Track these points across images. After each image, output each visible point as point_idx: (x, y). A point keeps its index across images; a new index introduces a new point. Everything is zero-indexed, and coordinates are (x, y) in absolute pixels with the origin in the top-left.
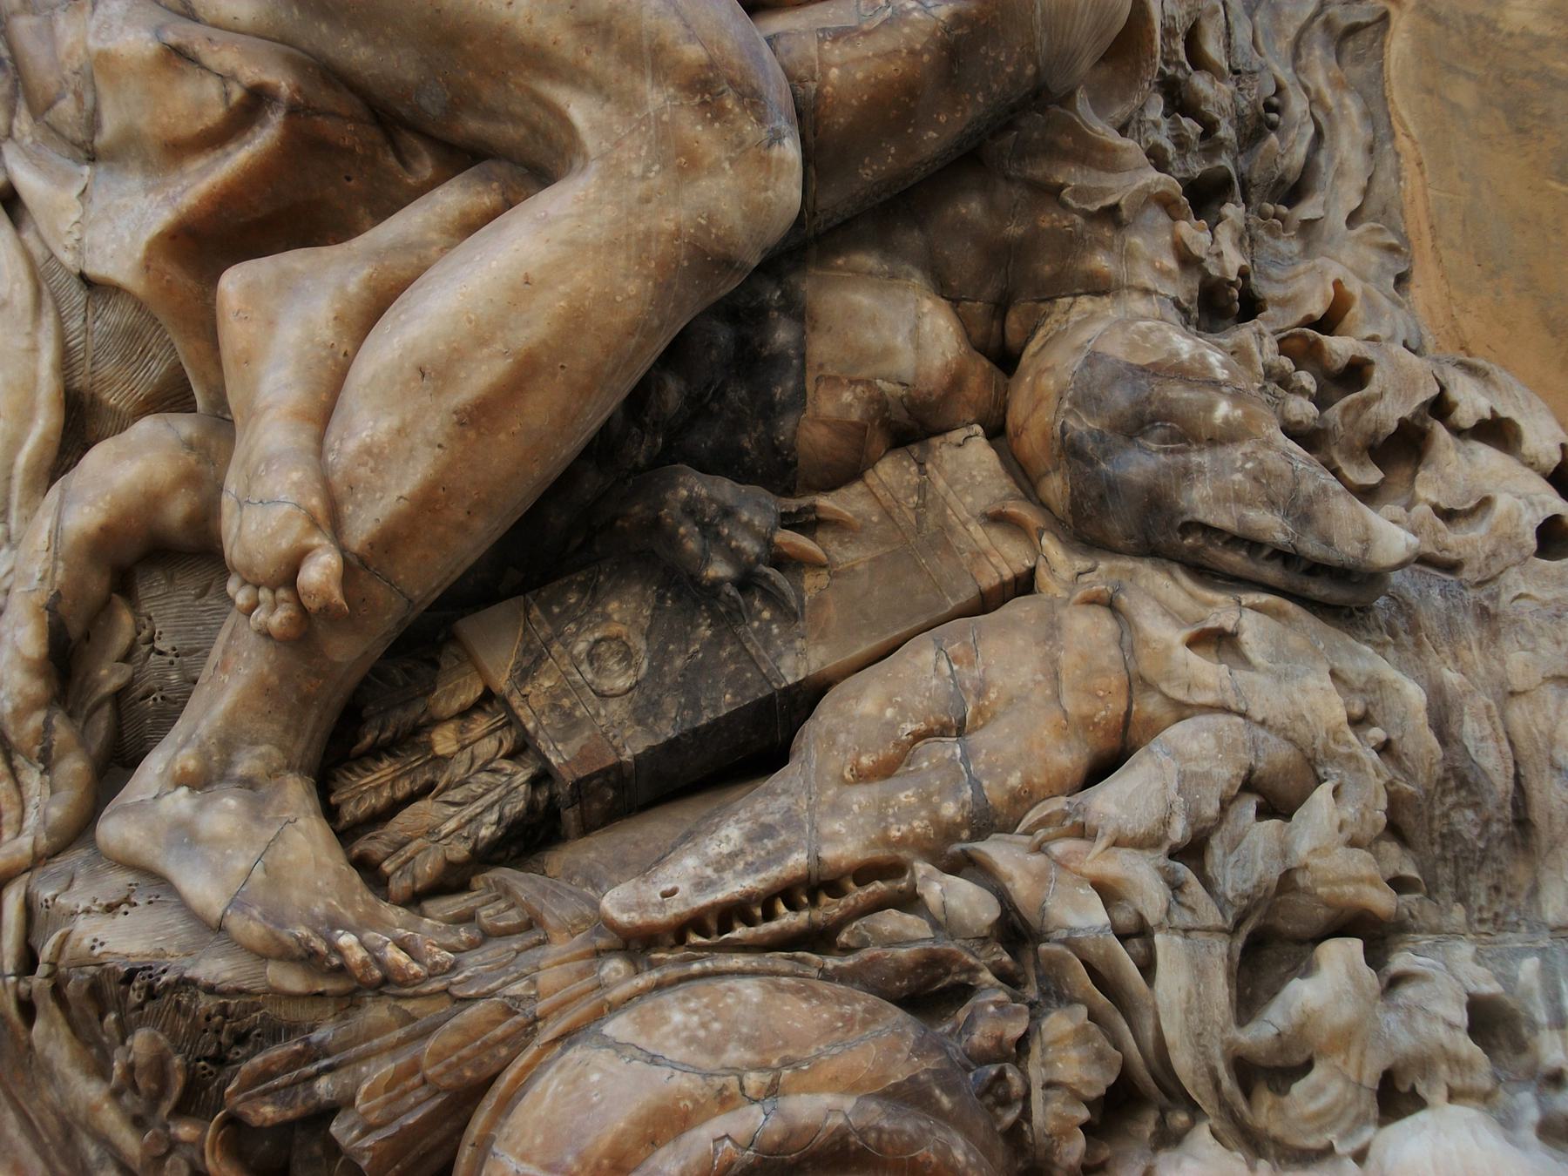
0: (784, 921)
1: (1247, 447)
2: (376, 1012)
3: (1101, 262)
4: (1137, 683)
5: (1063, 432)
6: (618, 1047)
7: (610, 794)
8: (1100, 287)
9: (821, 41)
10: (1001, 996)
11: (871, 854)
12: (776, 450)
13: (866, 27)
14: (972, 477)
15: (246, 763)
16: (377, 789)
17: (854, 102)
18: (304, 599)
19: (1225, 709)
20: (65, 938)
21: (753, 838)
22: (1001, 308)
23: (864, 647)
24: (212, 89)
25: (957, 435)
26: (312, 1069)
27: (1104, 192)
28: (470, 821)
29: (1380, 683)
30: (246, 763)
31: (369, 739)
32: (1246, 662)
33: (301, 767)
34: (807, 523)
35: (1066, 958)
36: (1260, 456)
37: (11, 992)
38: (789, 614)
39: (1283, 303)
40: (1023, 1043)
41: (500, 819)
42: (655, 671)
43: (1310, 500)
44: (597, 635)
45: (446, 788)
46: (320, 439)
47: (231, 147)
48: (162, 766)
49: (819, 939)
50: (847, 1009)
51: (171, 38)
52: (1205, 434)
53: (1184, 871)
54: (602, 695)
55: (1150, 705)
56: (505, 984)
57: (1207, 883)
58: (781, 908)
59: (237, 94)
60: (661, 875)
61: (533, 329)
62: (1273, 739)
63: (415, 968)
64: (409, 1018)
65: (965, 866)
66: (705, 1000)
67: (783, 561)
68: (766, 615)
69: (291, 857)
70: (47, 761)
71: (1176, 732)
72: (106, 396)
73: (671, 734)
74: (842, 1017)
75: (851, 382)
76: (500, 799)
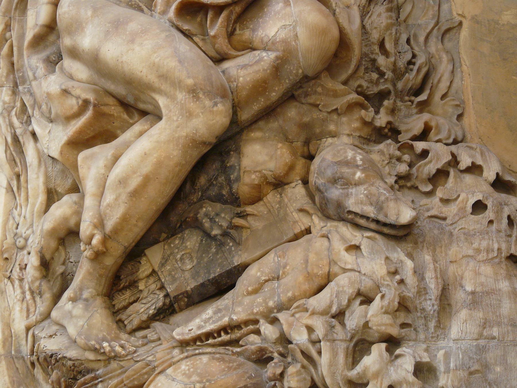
2: (114, 365)
3: (332, 127)
4: (332, 262)
7: (186, 300)
8: (334, 135)
9: (238, 69)
11: (248, 318)
12: (233, 194)
13: (251, 63)
15: (86, 294)
17: (248, 88)
21: (215, 313)
23: (258, 253)
25: (293, 185)
26: (97, 382)
28: (147, 308)
29: (402, 261)
30: (86, 294)
31: (122, 286)
33: (102, 295)
34: (243, 216)
35: (295, 349)
39: (407, 131)
40: (282, 375)
42: (199, 263)
44: (183, 253)
45: (142, 299)
47: (81, 117)
51: (63, 87)
52: (353, 183)
53: (334, 321)
54: (183, 270)
55: (335, 269)
56: (148, 357)
59: (80, 102)
61: (146, 169)
62: (367, 280)
64: (122, 367)
65: (274, 321)
67: (237, 228)
69: (94, 321)
70: (41, 294)
73: (202, 281)
76: (156, 302)
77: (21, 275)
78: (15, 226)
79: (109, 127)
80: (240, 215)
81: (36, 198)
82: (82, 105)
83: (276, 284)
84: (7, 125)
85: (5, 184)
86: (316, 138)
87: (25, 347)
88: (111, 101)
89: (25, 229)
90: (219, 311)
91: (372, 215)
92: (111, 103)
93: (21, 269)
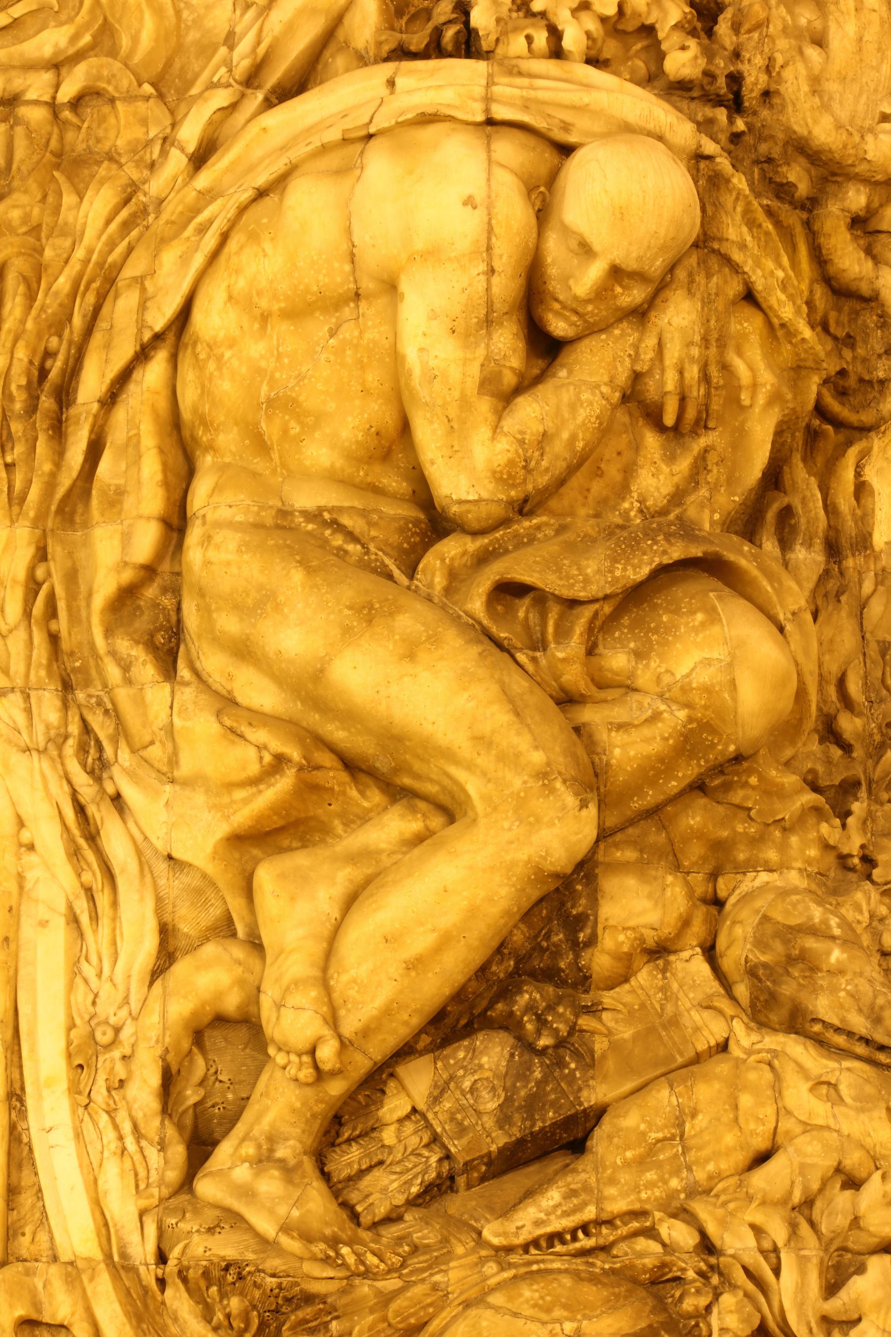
0: (583, 1243)
1: (848, 977)
4: (782, 1111)
5: (746, 962)
6: (496, 1309)
7: (483, 1168)
10: (698, 1284)
11: (630, 1207)
12: (580, 969)
14: (694, 981)
16: (350, 1165)
17: (629, 768)
18: (320, 1065)
22: (714, 876)
23: (629, 1086)
24: (252, 752)
25: (685, 955)
31: (346, 1135)
44: (476, 1077)
50: (616, 1290)
54: (479, 1114)
57: (812, 1224)
58: (580, 1235)
59: (267, 758)
61: (449, 919)
63: (382, 1266)
70: (162, 1146)
74: (614, 1294)
75: (624, 929)
78: (91, 998)
79: (320, 812)
82: (270, 764)
84: (60, 777)
85: (62, 907)
86: (735, 868)
87: (140, 1249)
88: (326, 759)
91: (863, 1032)
92: (328, 764)
93: (109, 1091)
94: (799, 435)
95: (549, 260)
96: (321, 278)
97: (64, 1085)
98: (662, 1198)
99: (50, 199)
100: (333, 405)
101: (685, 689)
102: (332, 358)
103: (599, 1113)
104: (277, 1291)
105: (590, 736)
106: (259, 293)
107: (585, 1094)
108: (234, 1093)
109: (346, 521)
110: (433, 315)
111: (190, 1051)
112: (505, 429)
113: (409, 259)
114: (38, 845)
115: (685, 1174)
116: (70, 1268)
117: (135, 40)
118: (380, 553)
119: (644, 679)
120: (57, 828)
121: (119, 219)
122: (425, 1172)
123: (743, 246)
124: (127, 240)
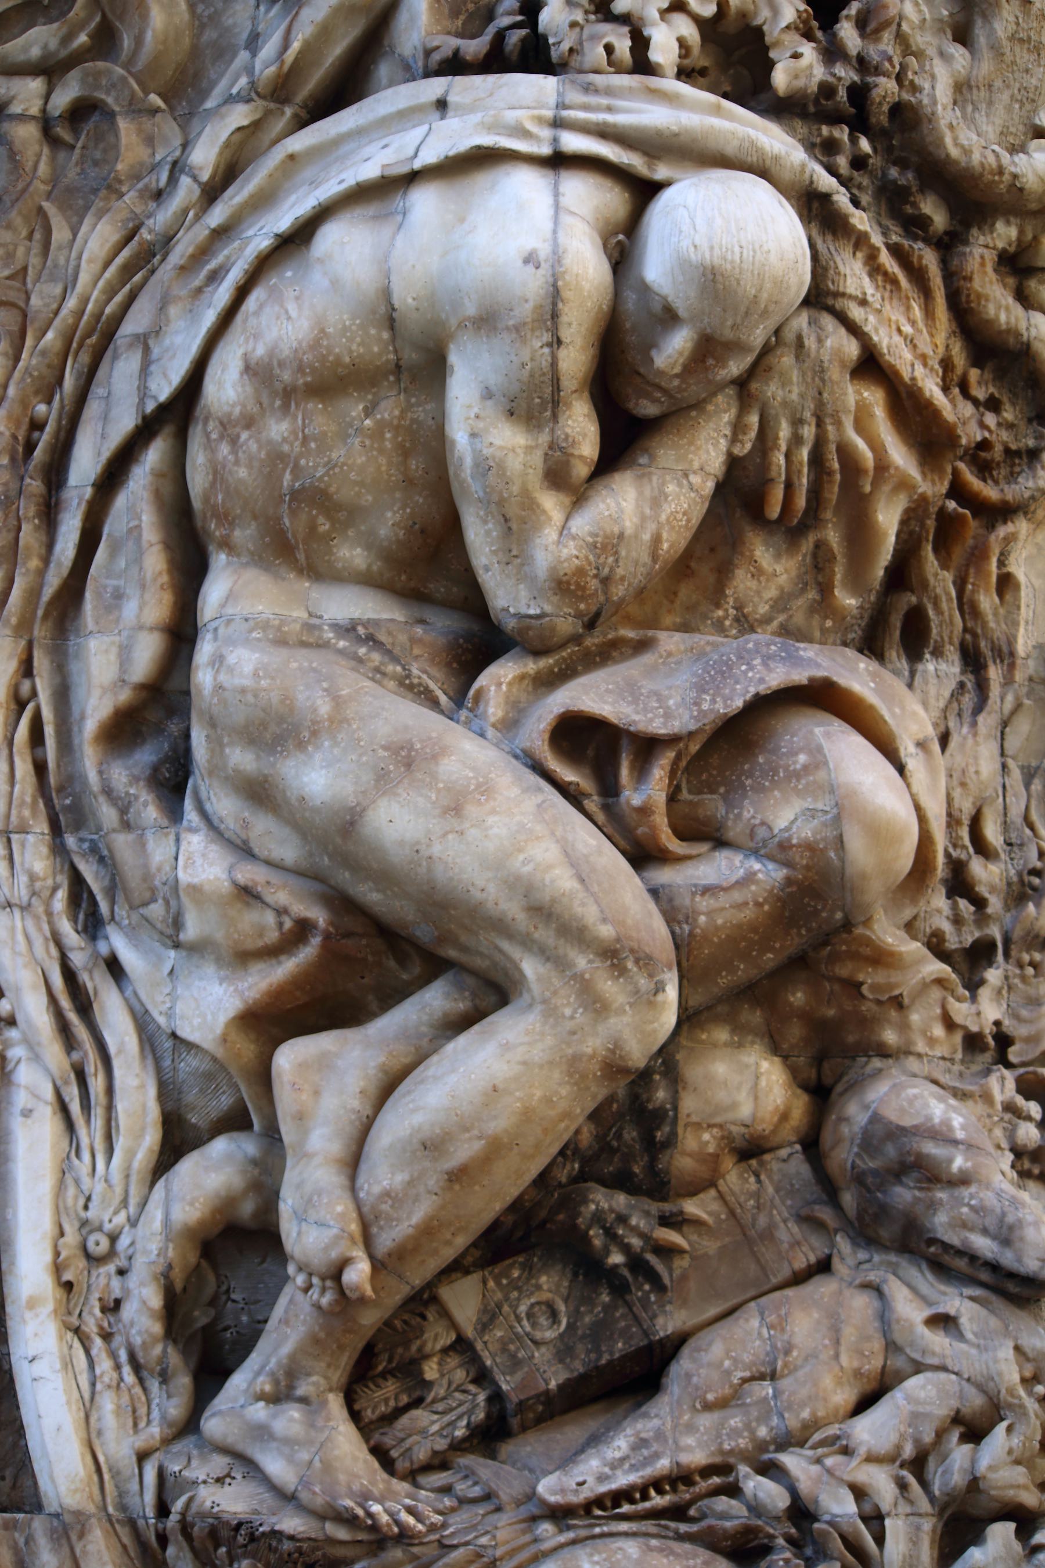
0: (653, 1502)
3: (890, 1037)
4: (892, 1347)
5: (853, 1167)
7: (540, 1408)
11: (710, 1461)
14: (792, 1185)
17: (716, 939)
18: (347, 1292)
19: (944, 1368)
20: (191, 1500)
23: (712, 1312)
25: (784, 1153)
27: (891, 987)
28: (449, 1424)
30: (303, 1389)
31: (380, 1368)
32: (960, 1336)
35: (829, 1533)
36: (981, 1195)
37: (152, 1529)
38: (659, 1286)
41: (468, 1424)
42: (569, 1326)
43: (1011, 1228)
44: (533, 1300)
45: (434, 1401)
46: (353, 1178)
47: (283, 958)
48: (244, 1385)
49: (678, 1512)
52: (944, 1177)
54: (536, 1343)
55: (898, 1362)
56: (476, 1537)
58: (653, 1493)
59: (288, 924)
60: (575, 1471)
61: (499, 1124)
63: (420, 1527)
65: (769, 1469)
66: (604, 1555)
68: (647, 1287)
70: (165, 1377)
71: (913, 1383)
72: (189, 1116)
73: (581, 1370)
77: (106, 1324)
78: (81, 1202)
80: (666, 1221)
81: (139, 1136)
82: (290, 931)
83: (766, 1389)
84: (46, 939)
85: (49, 1094)
87: (137, 1499)
89: (111, 1210)
90: (641, 1443)
93: (104, 1310)
94: (931, 524)
95: (628, 325)
96: (354, 347)
97: (50, 1306)
98: (747, 1450)
99: (37, 236)
100: (370, 498)
101: (784, 846)
102: (368, 442)
103: (677, 1343)
104: (296, 1555)
105: (671, 900)
106: (281, 364)
107: (660, 1321)
108: (250, 1314)
109: (382, 637)
110: (488, 394)
111: (198, 1265)
112: (574, 530)
113: (459, 325)
114: (19, 1018)
115: (775, 1421)
116: (55, 1523)
117: (139, 41)
118: (424, 676)
119: (735, 831)
120: (44, 999)
121: (119, 260)
122: (470, 1412)
123: (863, 302)
124: (128, 287)
